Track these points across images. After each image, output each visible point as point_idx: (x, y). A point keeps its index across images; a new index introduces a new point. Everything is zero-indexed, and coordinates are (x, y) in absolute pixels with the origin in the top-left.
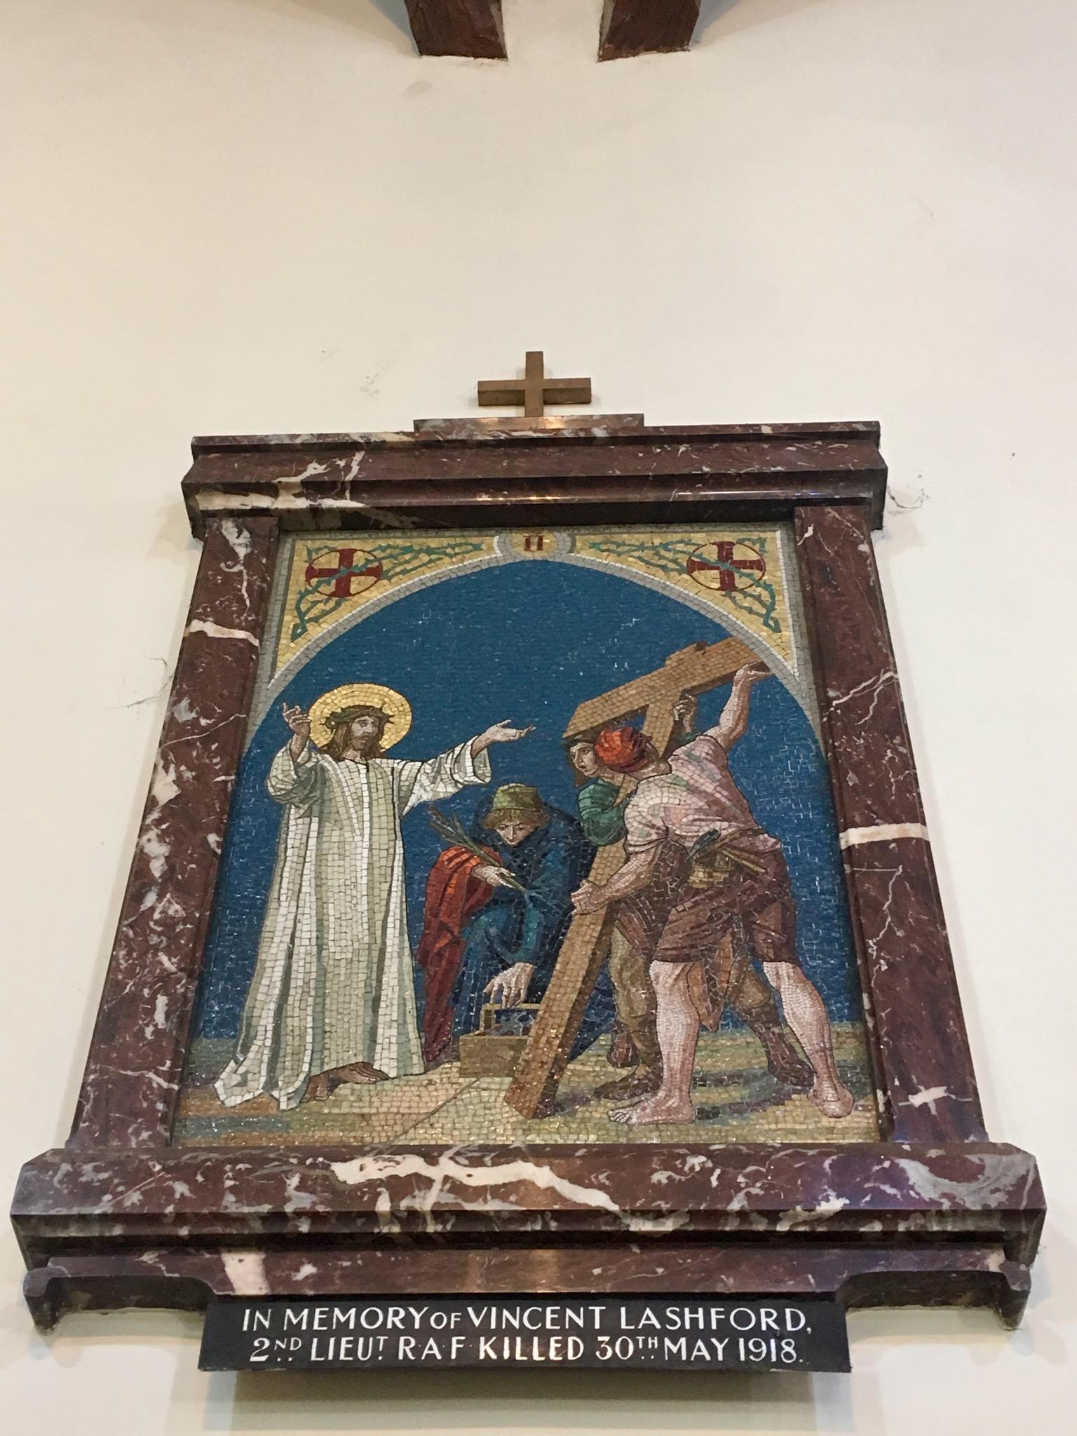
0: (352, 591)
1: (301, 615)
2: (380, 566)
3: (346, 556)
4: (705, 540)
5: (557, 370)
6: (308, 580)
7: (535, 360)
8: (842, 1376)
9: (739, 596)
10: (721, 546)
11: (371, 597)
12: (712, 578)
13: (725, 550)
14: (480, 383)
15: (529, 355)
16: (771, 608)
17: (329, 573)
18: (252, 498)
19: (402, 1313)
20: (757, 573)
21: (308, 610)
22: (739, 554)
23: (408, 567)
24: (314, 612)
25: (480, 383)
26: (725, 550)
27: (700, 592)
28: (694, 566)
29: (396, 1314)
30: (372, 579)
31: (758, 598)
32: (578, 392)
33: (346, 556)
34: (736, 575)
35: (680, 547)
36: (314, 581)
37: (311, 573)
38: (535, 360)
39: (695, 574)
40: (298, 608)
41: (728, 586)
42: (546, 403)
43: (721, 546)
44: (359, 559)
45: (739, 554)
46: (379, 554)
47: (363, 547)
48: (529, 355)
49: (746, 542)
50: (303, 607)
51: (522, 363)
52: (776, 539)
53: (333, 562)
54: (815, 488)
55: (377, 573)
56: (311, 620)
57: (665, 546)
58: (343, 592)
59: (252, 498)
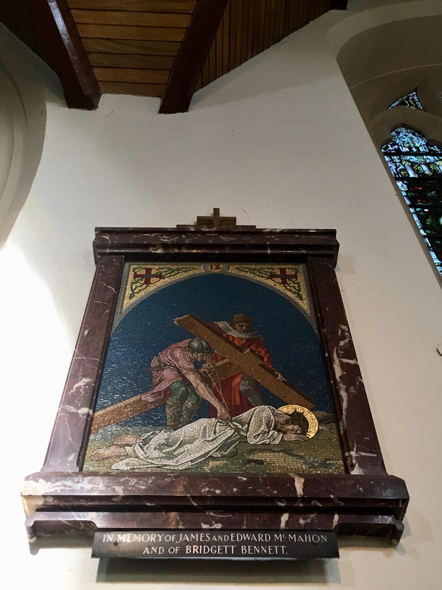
1: (132, 290)
2: (161, 275)
3: (148, 271)
4: (276, 269)
6: (135, 277)
8: (336, 559)
10: (281, 269)
11: (156, 285)
12: (280, 280)
13: (283, 271)
16: (299, 290)
17: (142, 276)
19: (155, 536)
21: (135, 289)
22: (288, 272)
24: (137, 290)
26: (283, 271)
28: (272, 276)
29: (154, 536)
31: (294, 287)
33: (148, 271)
35: (268, 270)
36: (136, 279)
37: (136, 276)
40: (131, 287)
41: (284, 283)
43: (281, 269)
45: (288, 272)
46: (162, 270)
47: (155, 268)
50: (134, 287)
51: (212, 212)
52: (301, 268)
53: (143, 272)
55: (160, 276)
56: (136, 293)
57: (262, 269)
58: (148, 282)
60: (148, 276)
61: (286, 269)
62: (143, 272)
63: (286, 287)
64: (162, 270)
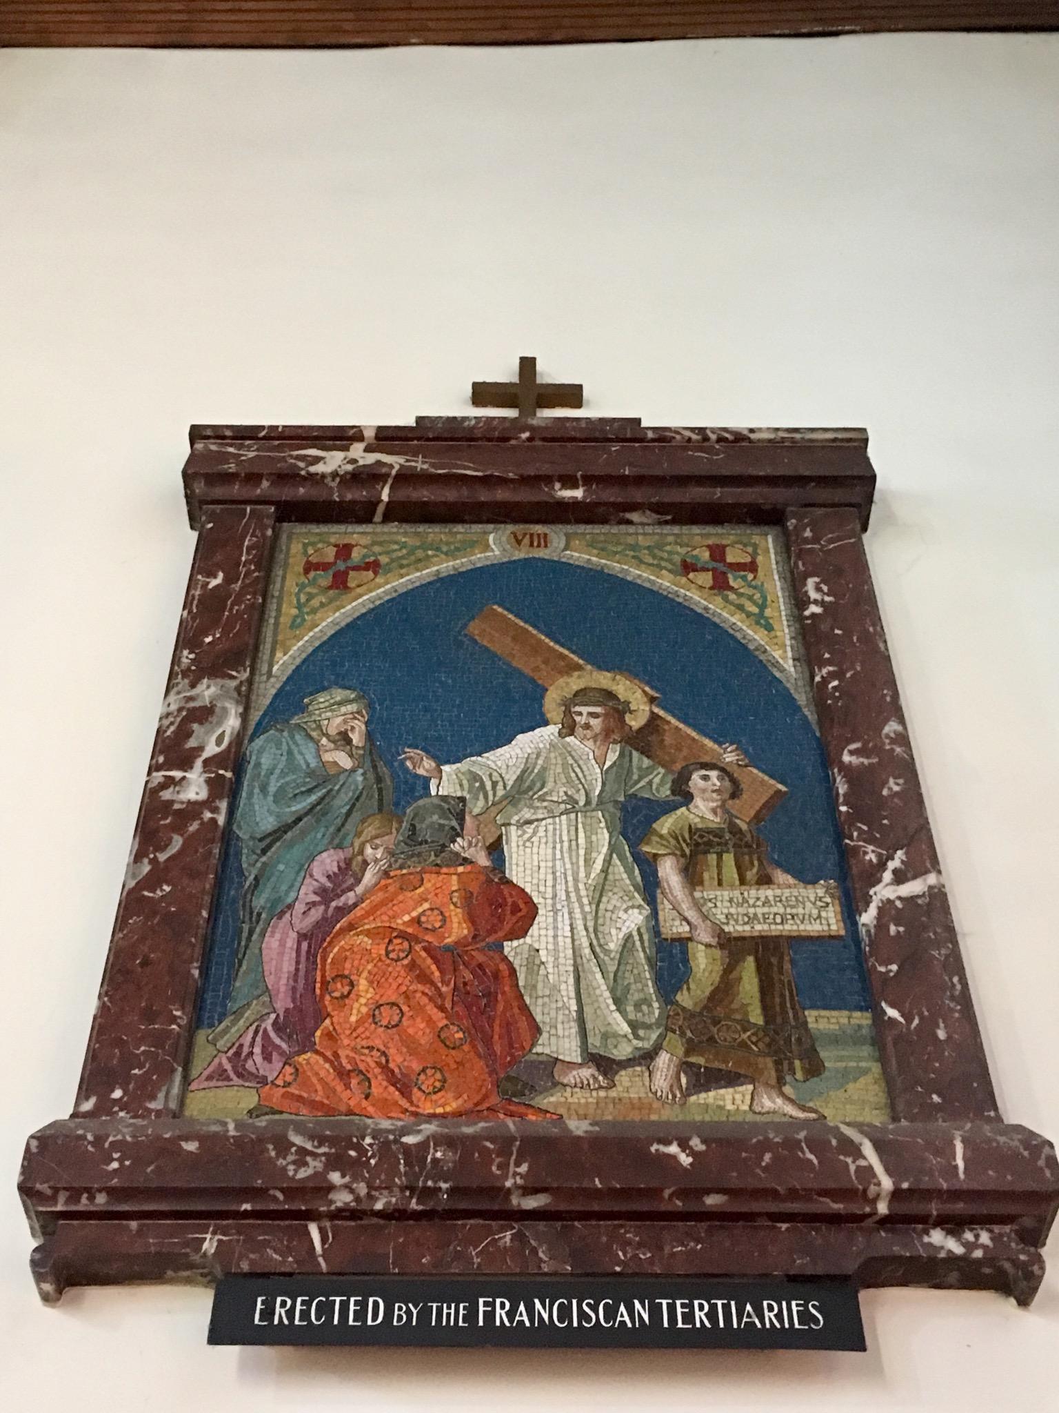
0: (351, 584)
1: (299, 606)
3: (344, 551)
4: (697, 541)
5: (551, 372)
7: (528, 365)
9: (732, 596)
12: (706, 579)
13: (718, 553)
14: (475, 385)
15: (523, 359)
17: (324, 567)
18: (251, 493)
20: (750, 576)
22: (734, 556)
23: (405, 562)
25: (475, 385)
26: (718, 553)
27: (695, 594)
28: (688, 567)
30: (370, 574)
31: (750, 598)
32: (572, 395)
34: (730, 576)
36: (312, 574)
38: (528, 365)
39: (691, 575)
41: (720, 585)
42: (540, 407)
44: (356, 555)
45: (734, 556)
48: (523, 359)
49: (737, 543)
52: (768, 545)
54: (810, 492)
55: (374, 566)
58: (340, 583)
59: (251, 493)
60: (341, 566)
61: (724, 547)
62: (330, 554)
63: (726, 599)
64: (377, 549)
